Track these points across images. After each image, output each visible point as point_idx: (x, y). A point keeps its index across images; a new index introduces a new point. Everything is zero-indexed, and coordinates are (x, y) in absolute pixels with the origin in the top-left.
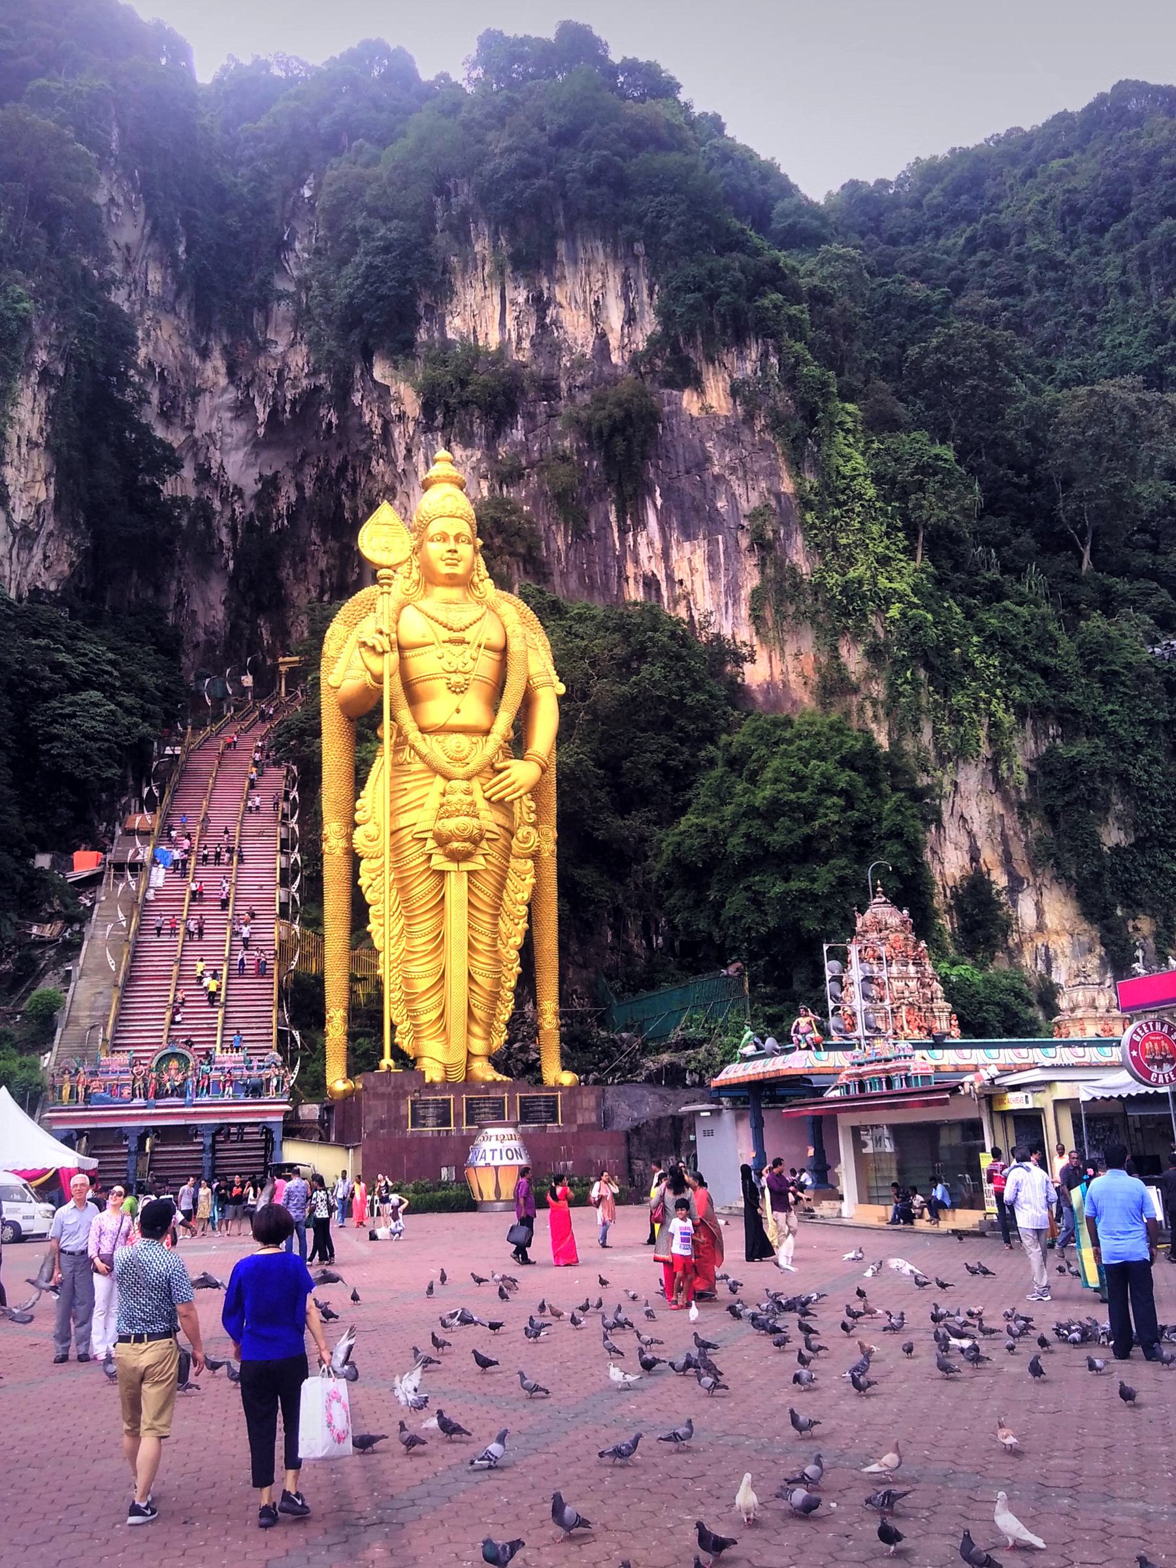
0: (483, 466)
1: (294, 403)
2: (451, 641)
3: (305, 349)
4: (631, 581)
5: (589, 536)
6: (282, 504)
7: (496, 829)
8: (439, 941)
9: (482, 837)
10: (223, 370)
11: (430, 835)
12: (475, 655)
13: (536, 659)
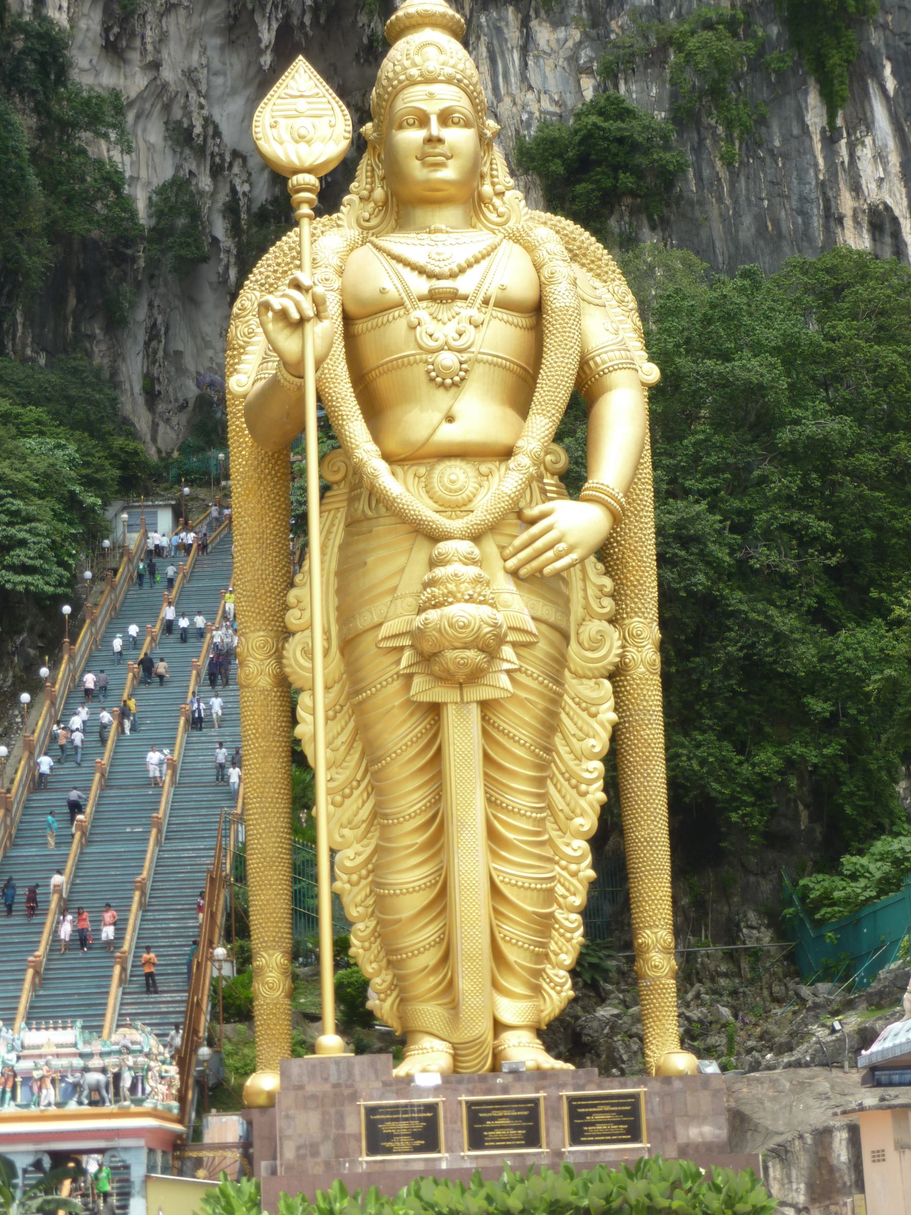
0: (585, 55)
2: (434, 297)
4: (848, 222)
5: (771, 151)
7: (532, 626)
9: (501, 640)
11: (407, 642)
12: (478, 317)
13: (607, 323)
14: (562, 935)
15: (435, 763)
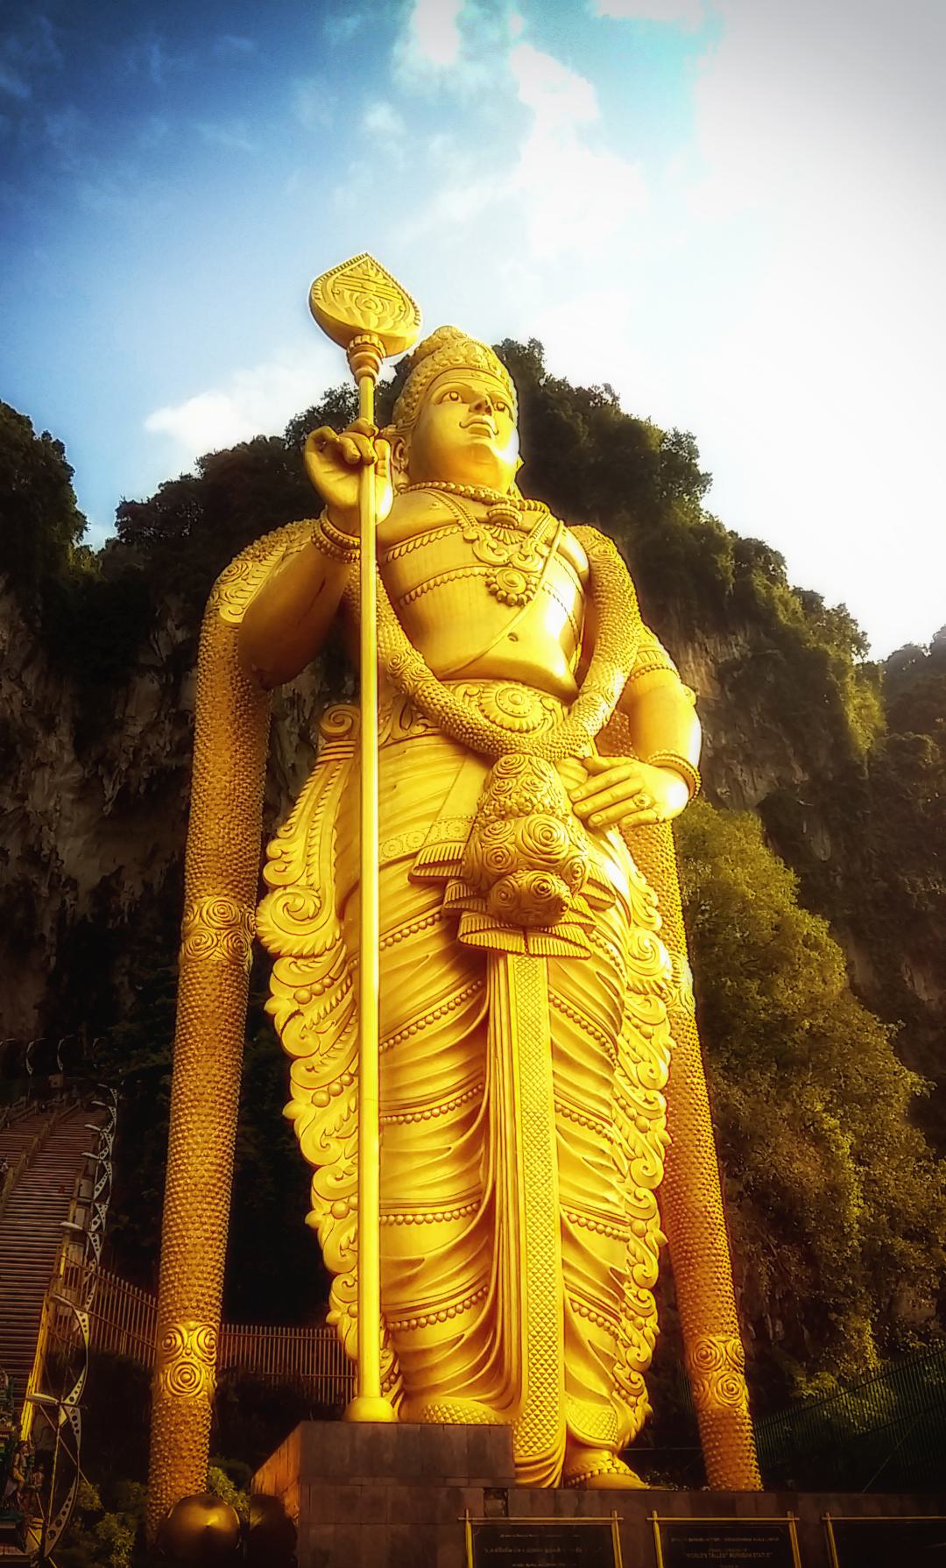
1: (150, 782)
3: (168, 727)
6: (124, 900)
8: (477, 1127)
10: (69, 747)
14: (632, 1319)
15: (476, 1042)
